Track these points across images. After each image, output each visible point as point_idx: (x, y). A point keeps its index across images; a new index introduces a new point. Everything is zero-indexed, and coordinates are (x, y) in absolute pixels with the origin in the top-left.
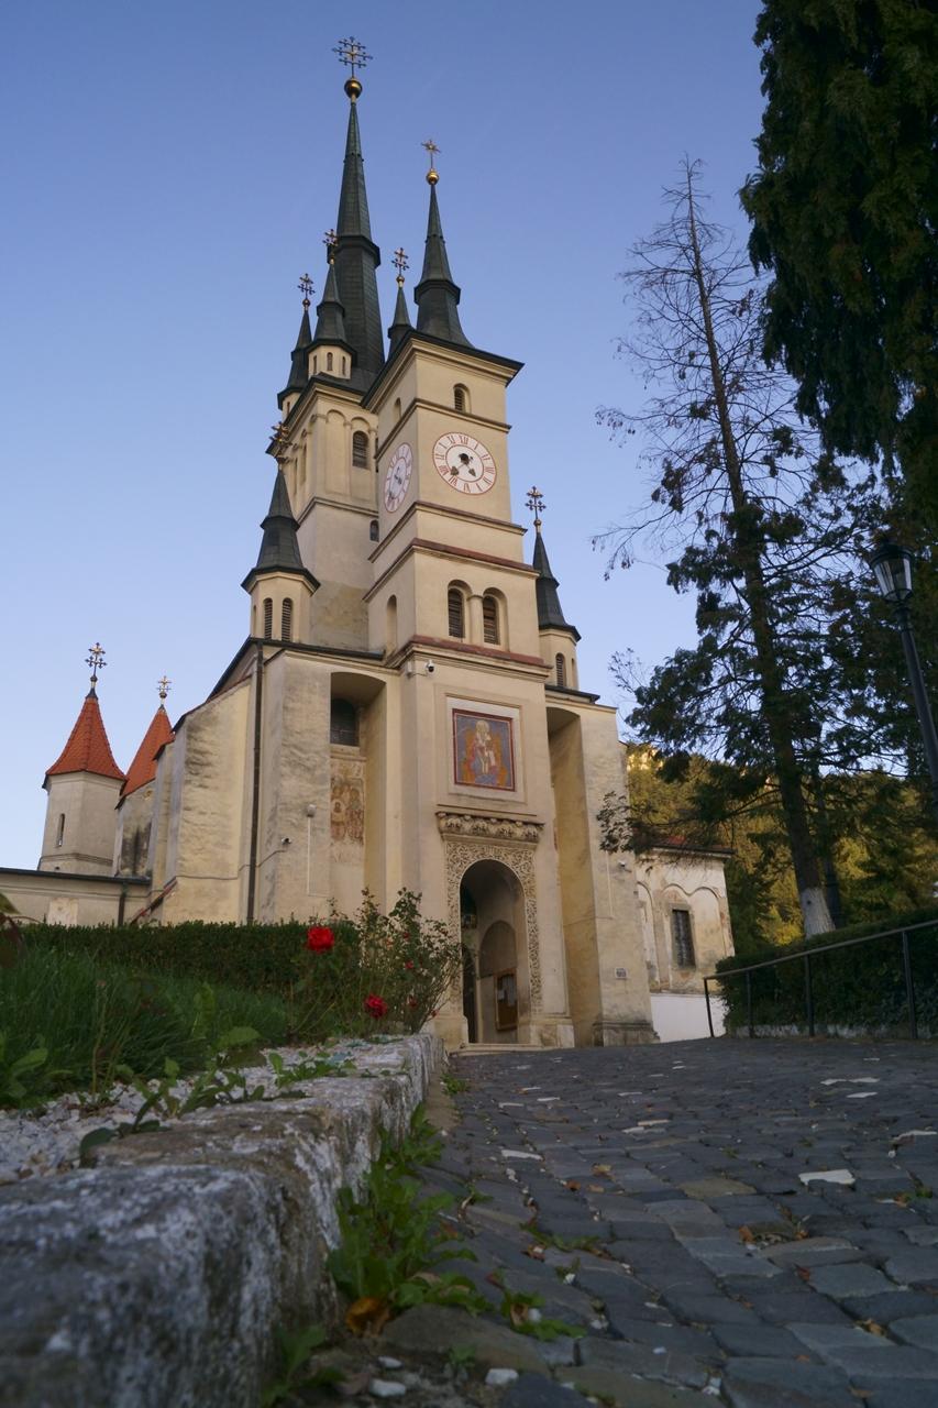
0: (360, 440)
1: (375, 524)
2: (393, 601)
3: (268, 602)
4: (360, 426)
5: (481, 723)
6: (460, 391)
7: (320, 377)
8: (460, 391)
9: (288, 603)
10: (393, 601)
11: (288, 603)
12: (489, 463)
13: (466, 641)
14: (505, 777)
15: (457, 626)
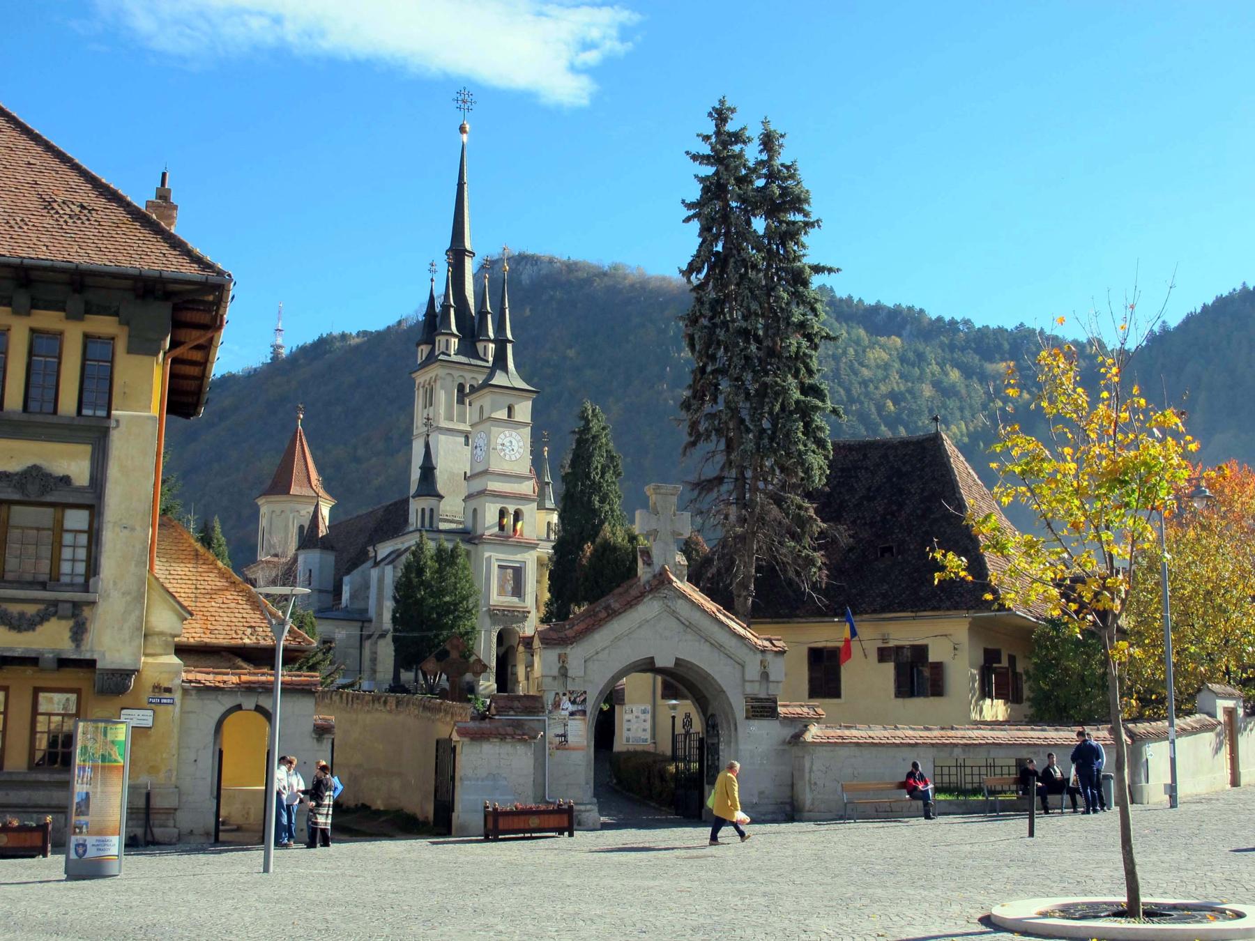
0: (461, 388)
1: (467, 438)
2: (475, 510)
3: (423, 510)
4: (462, 381)
5: (510, 571)
6: (510, 409)
7: (441, 357)
8: (510, 409)
9: (432, 510)
10: (475, 510)
11: (432, 510)
12: (521, 444)
13: (505, 534)
14: (518, 591)
15: (502, 527)
